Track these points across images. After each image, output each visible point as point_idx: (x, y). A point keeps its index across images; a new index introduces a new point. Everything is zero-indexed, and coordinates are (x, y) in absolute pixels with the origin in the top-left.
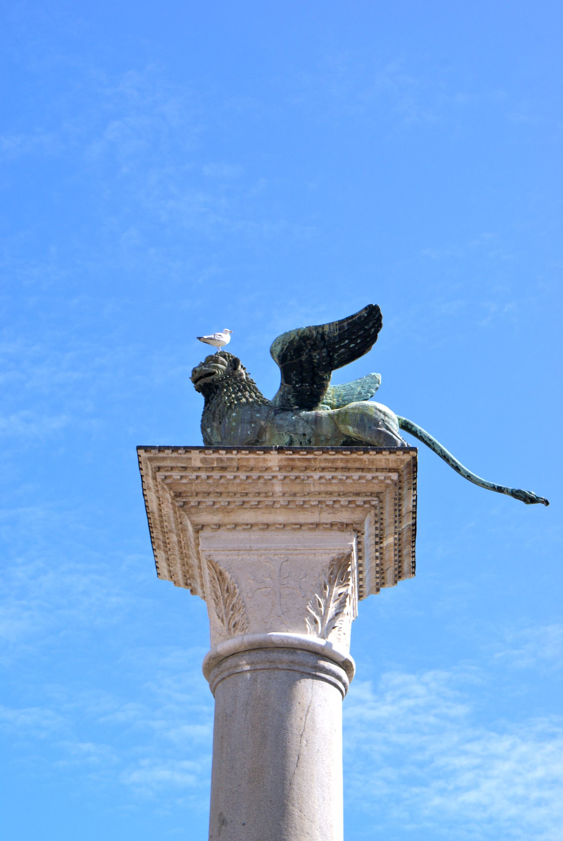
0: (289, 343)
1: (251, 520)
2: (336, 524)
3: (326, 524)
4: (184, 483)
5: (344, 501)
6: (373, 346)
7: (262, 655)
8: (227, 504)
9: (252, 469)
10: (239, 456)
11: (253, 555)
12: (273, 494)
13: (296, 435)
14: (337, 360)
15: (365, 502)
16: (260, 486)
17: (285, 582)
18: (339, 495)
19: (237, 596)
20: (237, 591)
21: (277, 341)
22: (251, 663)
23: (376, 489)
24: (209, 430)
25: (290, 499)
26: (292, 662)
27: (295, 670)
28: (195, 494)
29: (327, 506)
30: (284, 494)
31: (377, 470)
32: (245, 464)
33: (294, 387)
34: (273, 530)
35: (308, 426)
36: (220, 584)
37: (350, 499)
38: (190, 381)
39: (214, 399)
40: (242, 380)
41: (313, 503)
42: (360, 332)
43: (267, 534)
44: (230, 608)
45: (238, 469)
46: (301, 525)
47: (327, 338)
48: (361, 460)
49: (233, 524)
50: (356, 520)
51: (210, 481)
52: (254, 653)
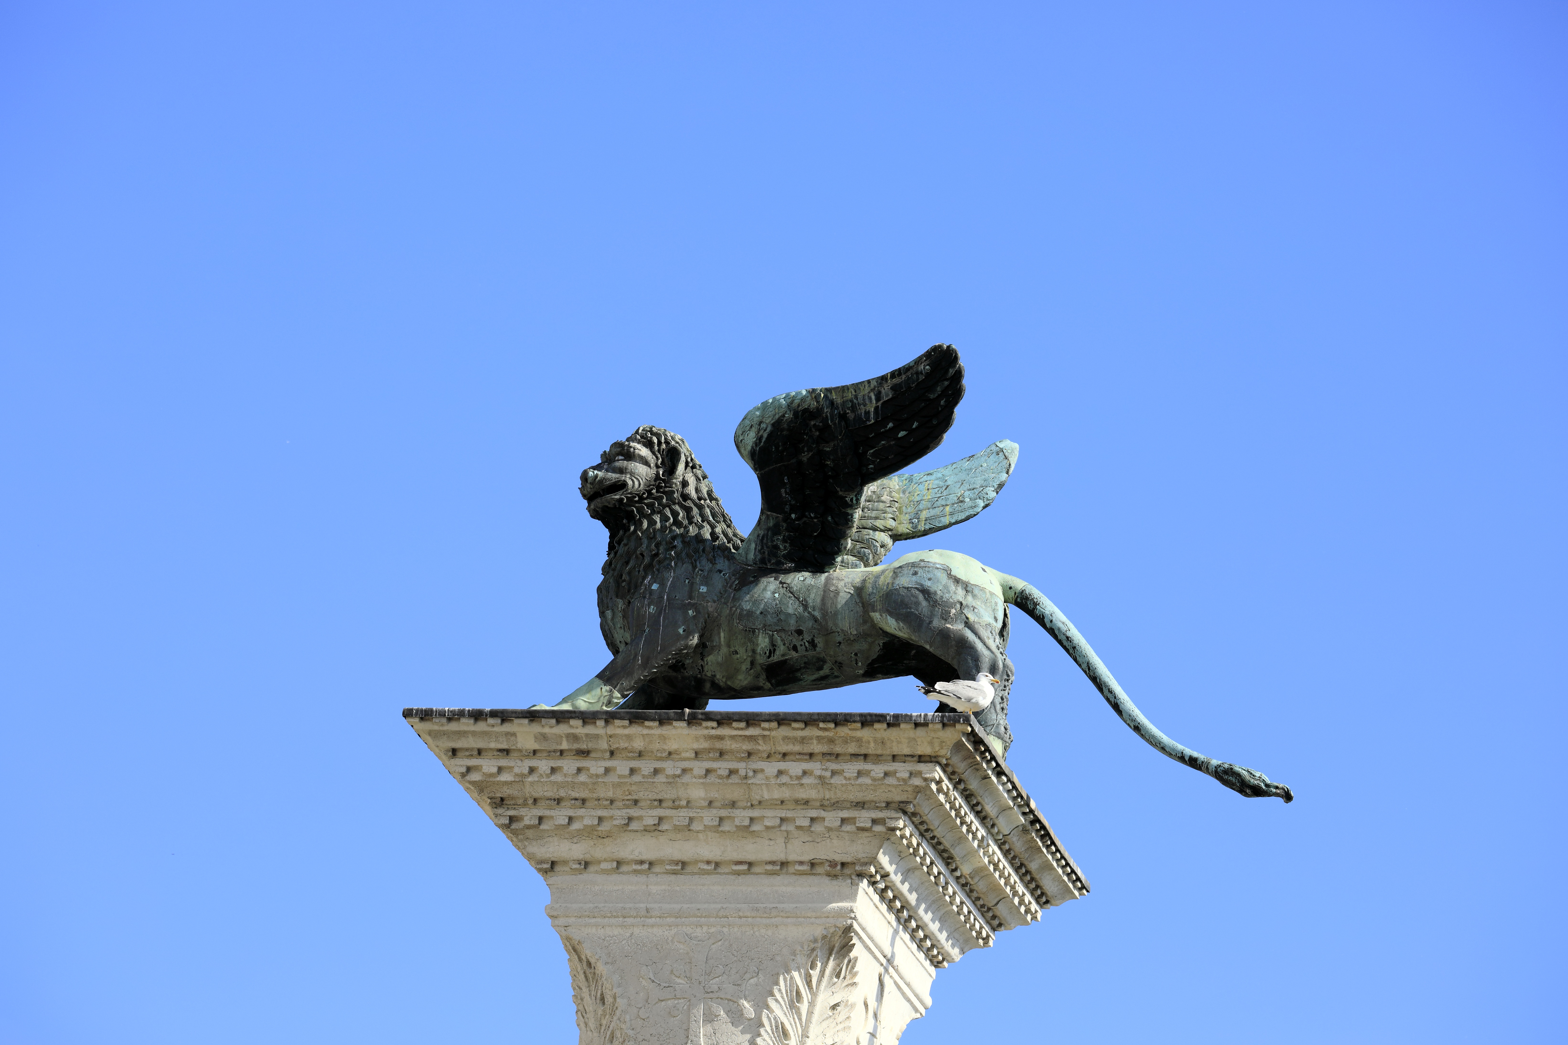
0: (773, 425)
1: (649, 855)
2: (822, 863)
3: (801, 863)
4: (506, 783)
5: (832, 818)
6: (945, 436)
8: (596, 822)
9: (640, 754)
10: (610, 730)
11: (653, 926)
12: (688, 802)
14: (873, 463)
17: (715, 988)
18: (823, 807)
21: (747, 422)
23: (897, 796)
24: (609, 614)
25: (724, 813)
28: (530, 802)
29: (799, 828)
30: (710, 803)
31: (894, 758)
32: (626, 745)
33: (787, 519)
34: (696, 874)
35: (806, 614)
37: (845, 814)
38: (647, 425)
40: (685, 497)
41: (768, 823)
42: (919, 404)
43: (684, 884)
45: (612, 753)
46: (750, 864)
47: (851, 416)
48: (859, 740)
49: (613, 860)
50: (860, 856)
51: (558, 778)
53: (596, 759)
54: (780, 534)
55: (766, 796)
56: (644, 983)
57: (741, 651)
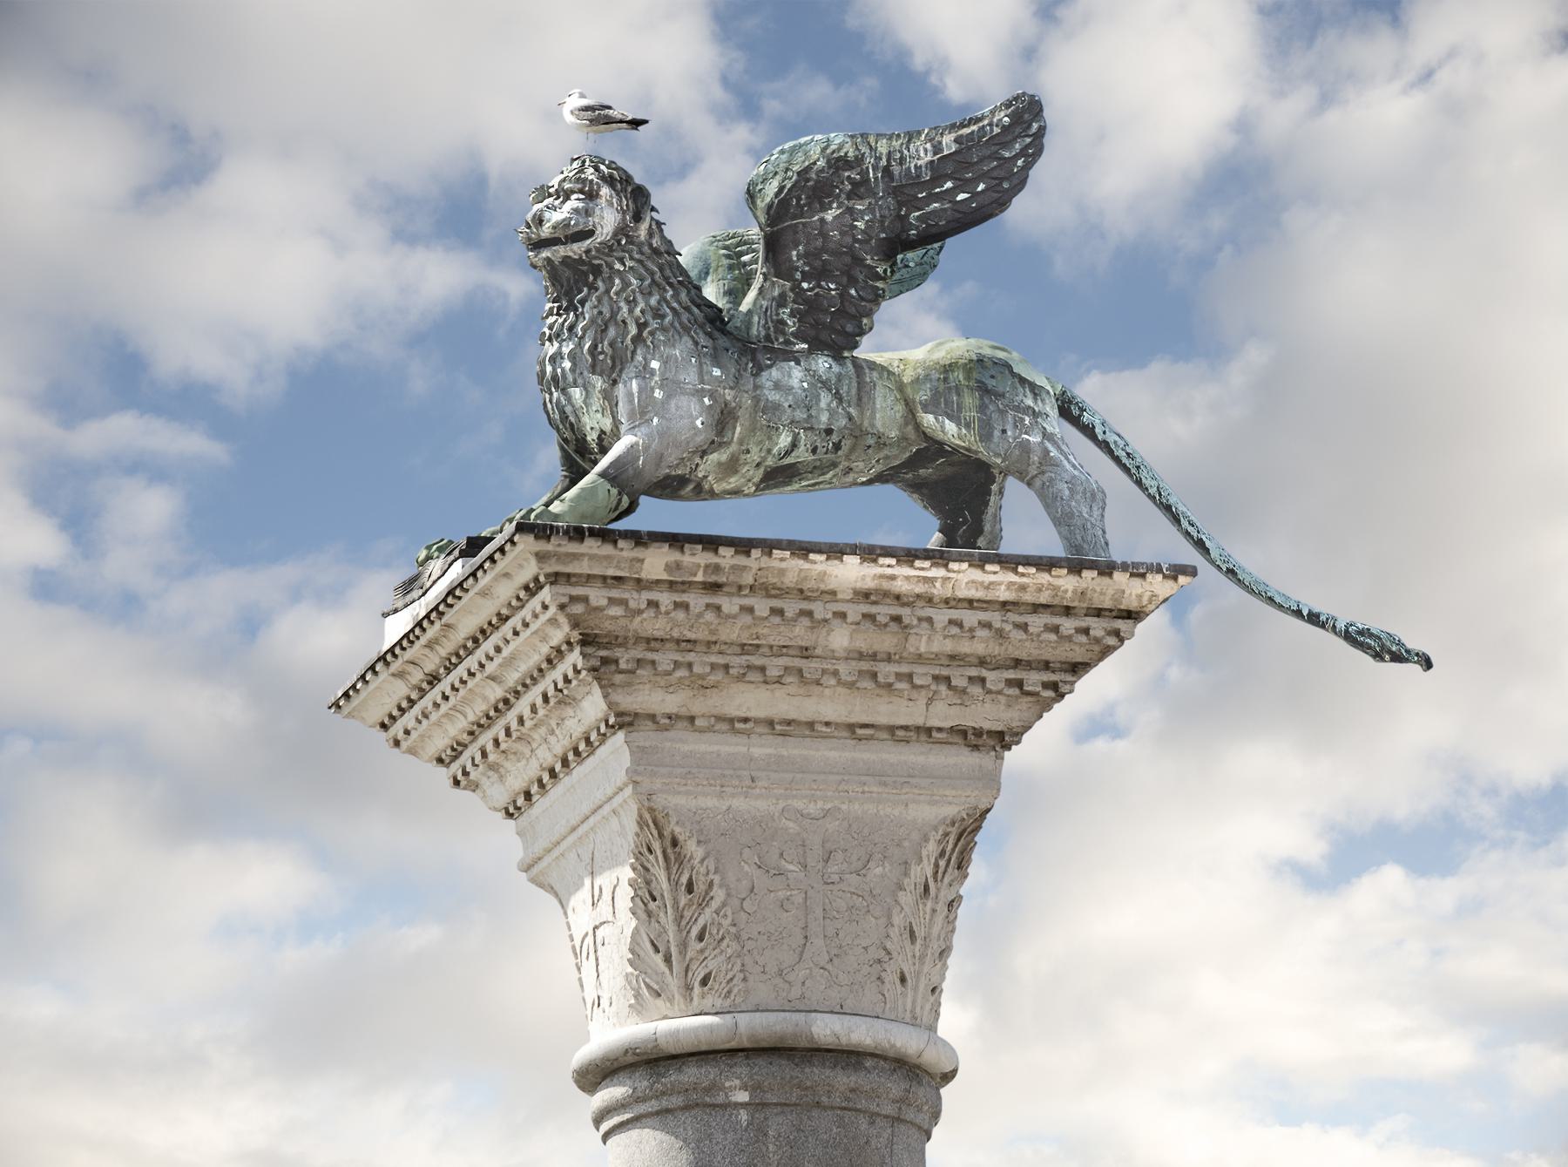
3: (940, 730)
7: (783, 1070)
10: (765, 562)
13: (809, 433)
14: (917, 228)
15: (1045, 685)
16: (800, 633)
17: (835, 878)
18: (982, 662)
19: (715, 904)
20: (719, 895)
22: (754, 1088)
23: (1078, 655)
26: (852, 1090)
27: (859, 1110)
33: (796, 287)
36: (668, 868)
37: (1011, 674)
39: (587, 305)
43: (794, 749)
44: (695, 932)
47: (896, 169)
52: (761, 1061)
53: (730, 594)
54: (785, 306)
55: (922, 650)
56: (746, 868)
57: (754, 450)
